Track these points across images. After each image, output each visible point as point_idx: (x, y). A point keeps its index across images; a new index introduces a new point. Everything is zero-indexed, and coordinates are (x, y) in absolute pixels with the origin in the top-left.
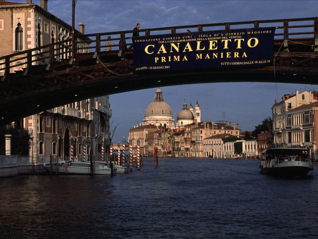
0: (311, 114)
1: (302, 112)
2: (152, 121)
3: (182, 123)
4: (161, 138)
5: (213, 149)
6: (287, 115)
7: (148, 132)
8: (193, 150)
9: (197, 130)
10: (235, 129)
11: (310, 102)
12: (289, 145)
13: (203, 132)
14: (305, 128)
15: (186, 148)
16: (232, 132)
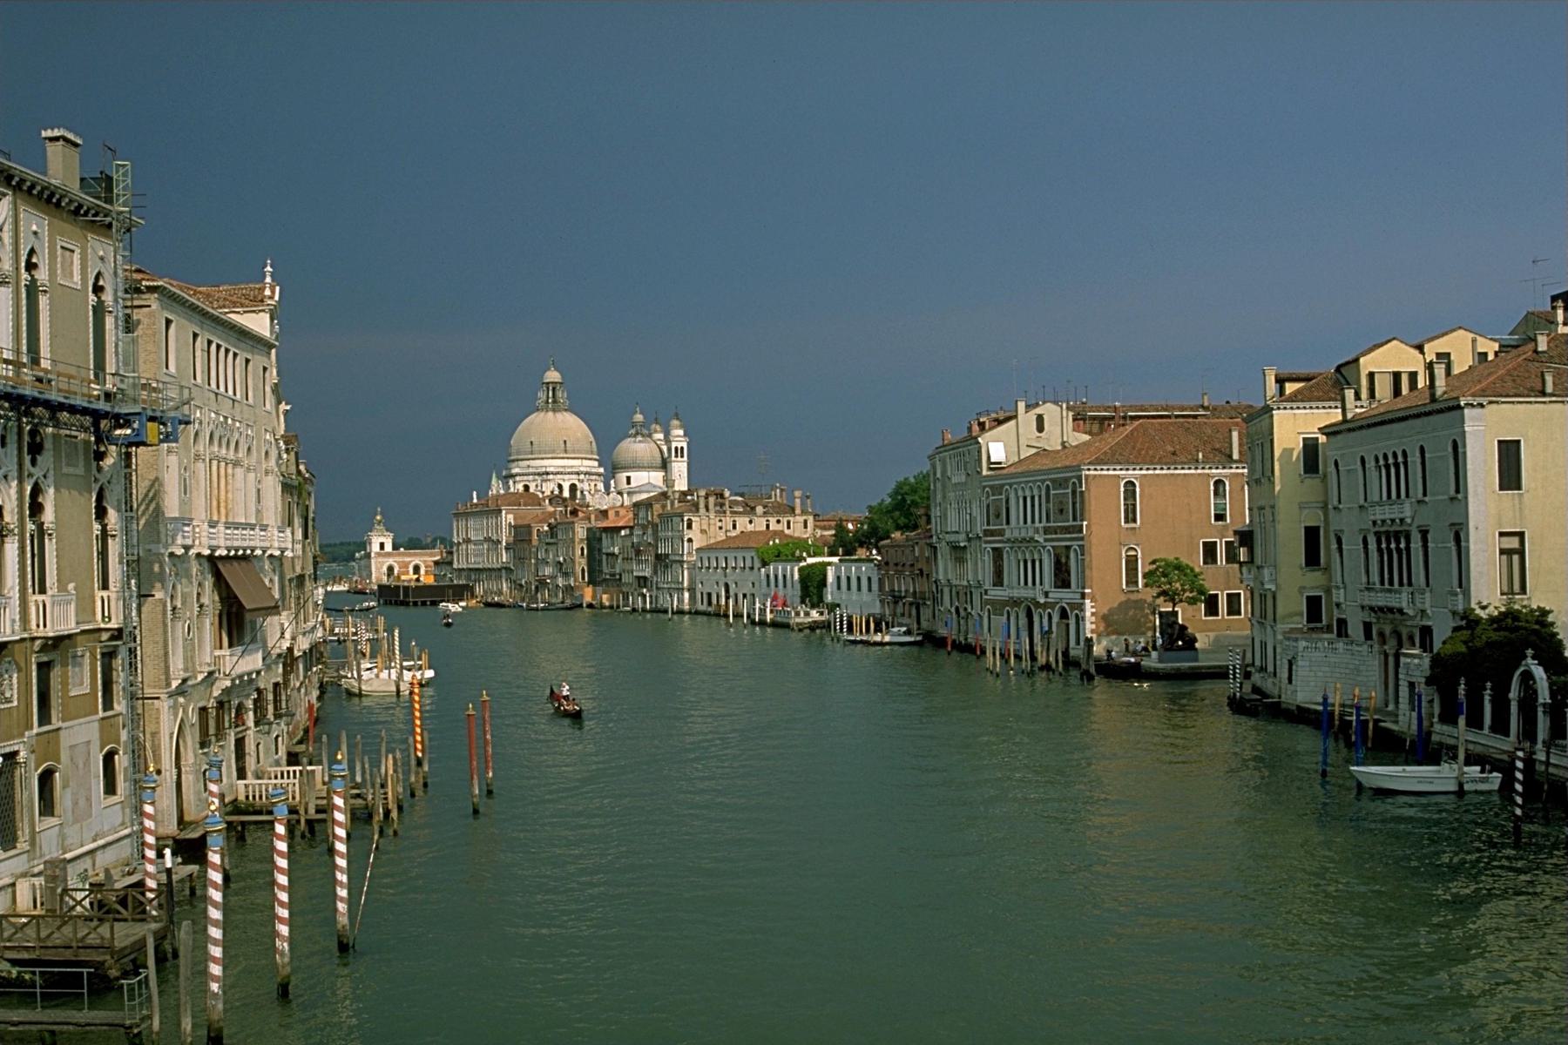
0: (1074, 492)
1: (1044, 481)
2: (531, 477)
3: (628, 479)
4: (552, 541)
5: (727, 587)
6: (987, 489)
7: (515, 519)
8: (661, 585)
9: (674, 519)
10: (798, 511)
11: (1063, 443)
12: (992, 593)
13: (694, 524)
14: (1053, 540)
15: (639, 578)
16: (789, 523)
